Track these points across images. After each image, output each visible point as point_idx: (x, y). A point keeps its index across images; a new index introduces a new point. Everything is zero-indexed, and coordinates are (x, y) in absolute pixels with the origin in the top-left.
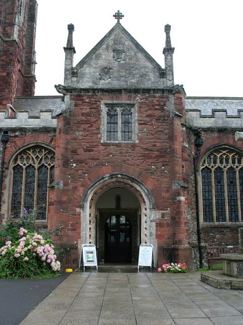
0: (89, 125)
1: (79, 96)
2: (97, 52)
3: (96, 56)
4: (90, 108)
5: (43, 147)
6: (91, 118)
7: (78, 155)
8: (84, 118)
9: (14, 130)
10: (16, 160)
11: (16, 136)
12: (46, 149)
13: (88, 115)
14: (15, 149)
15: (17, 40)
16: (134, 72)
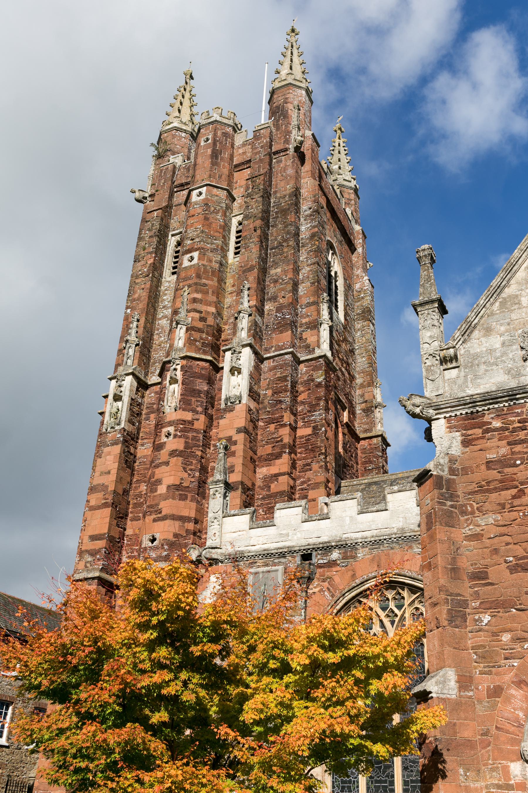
0: (514, 491)
2: (503, 295)
3: (503, 304)
4: (509, 444)
5: (403, 585)
6: (515, 470)
7: (492, 584)
8: (494, 474)
9: (326, 548)
11: (332, 564)
12: (413, 589)
13: (504, 463)
14: (332, 596)
15: (329, 354)
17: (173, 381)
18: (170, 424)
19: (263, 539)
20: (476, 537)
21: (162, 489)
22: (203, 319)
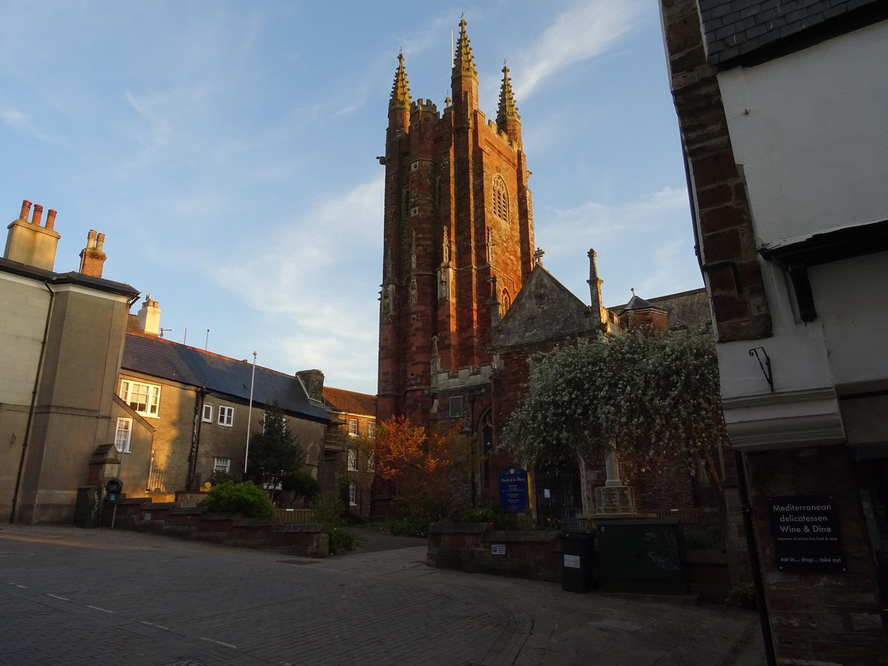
1: (508, 354)
9: (479, 387)
10: (485, 421)
11: (482, 394)
16: (559, 317)
17: (413, 288)
18: (414, 313)
19: (454, 384)
20: (507, 400)
21: (414, 349)
22: (425, 250)
